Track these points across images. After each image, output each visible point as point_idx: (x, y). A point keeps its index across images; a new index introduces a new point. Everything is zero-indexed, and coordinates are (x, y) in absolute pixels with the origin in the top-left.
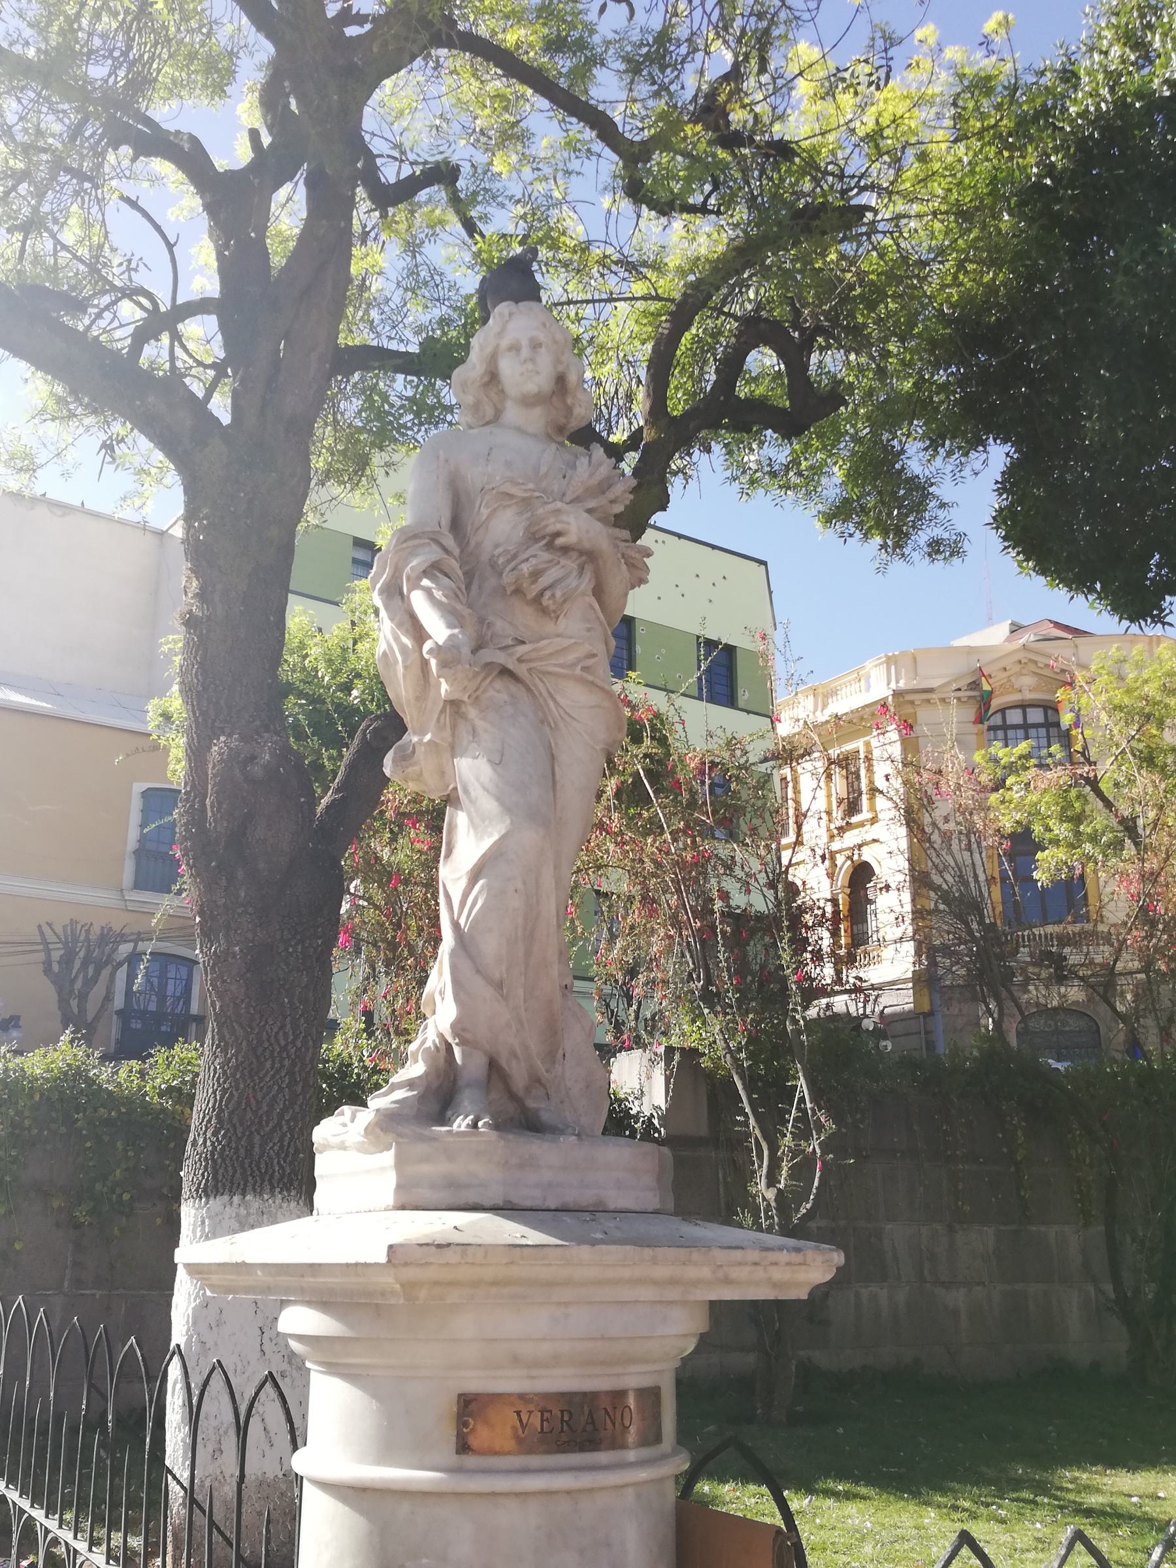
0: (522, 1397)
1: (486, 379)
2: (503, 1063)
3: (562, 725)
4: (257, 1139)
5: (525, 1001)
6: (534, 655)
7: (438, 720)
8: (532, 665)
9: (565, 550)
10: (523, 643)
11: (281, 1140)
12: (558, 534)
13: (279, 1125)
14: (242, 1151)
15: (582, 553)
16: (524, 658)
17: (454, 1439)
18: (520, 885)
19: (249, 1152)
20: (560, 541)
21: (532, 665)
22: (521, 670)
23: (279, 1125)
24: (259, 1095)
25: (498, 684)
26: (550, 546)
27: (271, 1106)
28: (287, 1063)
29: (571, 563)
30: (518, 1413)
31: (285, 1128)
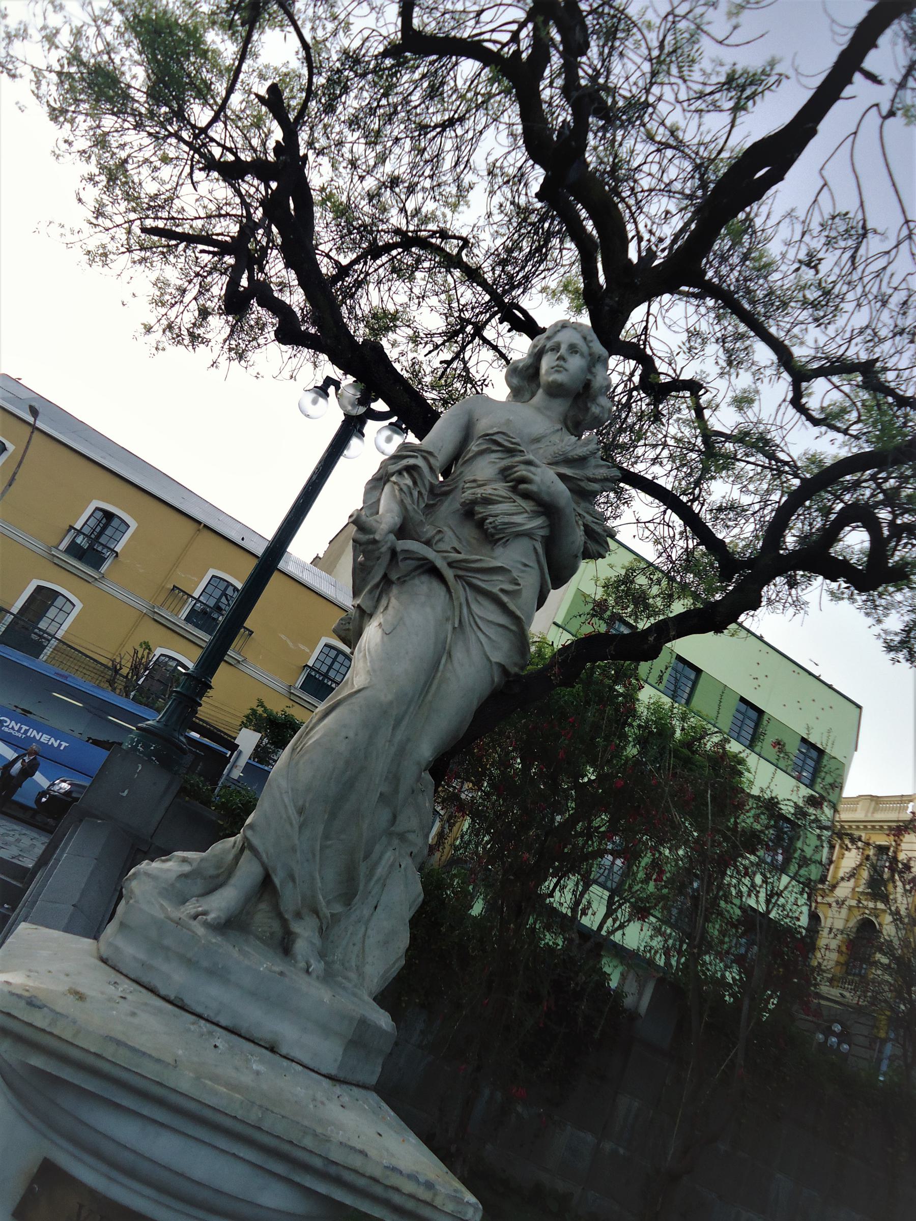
0: (92, 1193)
1: (531, 371)
2: (277, 881)
3: (468, 629)
5: (326, 836)
7: (371, 591)
8: (461, 573)
12: (523, 480)
17: (19, 1198)
18: (351, 734)
20: (522, 486)
21: (461, 573)
22: (449, 574)
25: (425, 578)
26: (514, 489)
29: (528, 505)
30: (81, 1206)
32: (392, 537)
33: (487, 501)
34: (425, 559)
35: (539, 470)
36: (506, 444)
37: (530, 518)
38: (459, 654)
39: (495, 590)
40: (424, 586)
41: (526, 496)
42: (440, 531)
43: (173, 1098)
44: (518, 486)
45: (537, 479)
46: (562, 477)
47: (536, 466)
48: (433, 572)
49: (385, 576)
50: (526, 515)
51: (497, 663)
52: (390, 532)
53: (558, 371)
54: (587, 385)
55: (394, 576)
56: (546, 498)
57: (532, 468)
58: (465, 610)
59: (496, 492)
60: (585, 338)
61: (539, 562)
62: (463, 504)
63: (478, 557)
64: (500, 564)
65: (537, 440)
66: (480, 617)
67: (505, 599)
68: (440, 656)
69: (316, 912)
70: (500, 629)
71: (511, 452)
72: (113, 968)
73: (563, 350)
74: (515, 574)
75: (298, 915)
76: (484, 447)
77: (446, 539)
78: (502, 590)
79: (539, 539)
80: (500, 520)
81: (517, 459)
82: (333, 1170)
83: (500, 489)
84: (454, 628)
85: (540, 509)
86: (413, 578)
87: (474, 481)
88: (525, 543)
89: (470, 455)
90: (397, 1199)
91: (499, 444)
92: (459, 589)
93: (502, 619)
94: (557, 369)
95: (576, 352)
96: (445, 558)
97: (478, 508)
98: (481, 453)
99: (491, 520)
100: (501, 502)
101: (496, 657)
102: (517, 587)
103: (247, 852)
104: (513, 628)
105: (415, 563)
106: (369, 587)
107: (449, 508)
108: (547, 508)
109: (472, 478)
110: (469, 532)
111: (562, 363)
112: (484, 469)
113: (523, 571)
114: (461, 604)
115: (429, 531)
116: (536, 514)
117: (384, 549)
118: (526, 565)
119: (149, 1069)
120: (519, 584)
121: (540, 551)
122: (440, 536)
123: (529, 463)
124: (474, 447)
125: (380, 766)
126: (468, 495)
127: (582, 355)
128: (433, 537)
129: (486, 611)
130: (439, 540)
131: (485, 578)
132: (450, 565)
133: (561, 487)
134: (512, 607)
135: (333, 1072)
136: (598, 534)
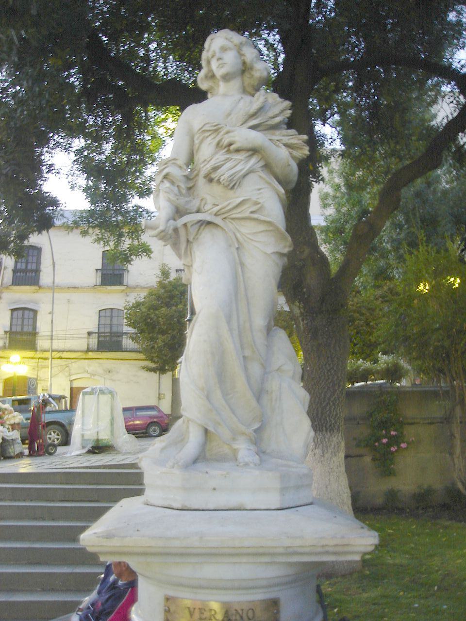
4: (320, 409)
6: (223, 210)
9: (238, 151)
10: (218, 205)
11: (330, 410)
12: (230, 144)
13: (328, 403)
14: (315, 414)
15: (248, 150)
16: (219, 213)
19: (317, 414)
20: (232, 147)
22: (218, 220)
23: (328, 403)
24: (320, 392)
26: (229, 152)
27: (325, 395)
28: (331, 377)
29: (241, 156)
31: (331, 404)
32: (172, 222)
33: (215, 169)
34: (200, 221)
35: (236, 132)
36: (211, 129)
37: (247, 162)
38: (248, 261)
39: (247, 214)
40: (206, 235)
41: (238, 151)
42: (202, 200)
43: (195, 551)
44: (229, 148)
45: (237, 139)
46: (253, 128)
47: (233, 131)
48: (209, 223)
49: (188, 241)
50: (242, 163)
51: (272, 253)
52: (168, 220)
53: (222, 67)
54: (244, 63)
55: (191, 239)
56: (250, 146)
57: (231, 134)
58: (238, 235)
59: (218, 161)
60: (227, 39)
61: (267, 182)
62: (205, 177)
63: (228, 202)
64: (241, 199)
65: (229, 114)
66: (248, 234)
67: (255, 216)
68: (238, 269)
69: (243, 434)
70: (263, 234)
71: (216, 131)
72: (151, 505)
73: (218, 55)
74: (254, 199)
75: (234, 439)
76: (201, 138)
77: (209, 201)
78: (252, 212)
79: (260, 170)
80: (226, 176)
81: (222, 133)
82: (291, 550)
83: (221, 156)
84: (237, 249)
85: (250, 153)
86: (201, 233)
87: (205, 160)
88: (251, 176)
89: (197, 146)
90: (331, 549)
91: (210, 131)
92: (229, 226)
93: (262, 228)
94: (221, 66)
95: (226, 50)
96: (211, 214)
97: (213, 176)
98: (201, 142)
99: (222, 178)
100: (223, 165)
101: (270, 250)
102: (259, 206)
103: (190, 422)
104: (271, 228)
105: (200, 224)
106: (183, 252)
107: (201, 181)
108: (254, 151)
109: (202, 160)
110: (217, 189)
111: (220, 62)
112: (206, 151)
113: (260, 193)
114: (234, 233)
115: (195, 204)
116: (251, 156)
117: (171, 231)
118: (260, 189)
119: (177, 543)
120: (260, 203)
121: (264, 176)
122: (203, 202)
123: (228, 132)
124: (197, 142)
125: (230, 346)
126: (203, 172)
127: (230, 49)
128: (200, 205)
129: (247, 229)
130: (204, 205)
131: (239, 210)
132: (216, 215)
133: (254, 134)
134: (263, 218)
135: (278, 506)
136: (297, 144)
